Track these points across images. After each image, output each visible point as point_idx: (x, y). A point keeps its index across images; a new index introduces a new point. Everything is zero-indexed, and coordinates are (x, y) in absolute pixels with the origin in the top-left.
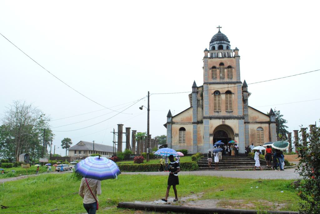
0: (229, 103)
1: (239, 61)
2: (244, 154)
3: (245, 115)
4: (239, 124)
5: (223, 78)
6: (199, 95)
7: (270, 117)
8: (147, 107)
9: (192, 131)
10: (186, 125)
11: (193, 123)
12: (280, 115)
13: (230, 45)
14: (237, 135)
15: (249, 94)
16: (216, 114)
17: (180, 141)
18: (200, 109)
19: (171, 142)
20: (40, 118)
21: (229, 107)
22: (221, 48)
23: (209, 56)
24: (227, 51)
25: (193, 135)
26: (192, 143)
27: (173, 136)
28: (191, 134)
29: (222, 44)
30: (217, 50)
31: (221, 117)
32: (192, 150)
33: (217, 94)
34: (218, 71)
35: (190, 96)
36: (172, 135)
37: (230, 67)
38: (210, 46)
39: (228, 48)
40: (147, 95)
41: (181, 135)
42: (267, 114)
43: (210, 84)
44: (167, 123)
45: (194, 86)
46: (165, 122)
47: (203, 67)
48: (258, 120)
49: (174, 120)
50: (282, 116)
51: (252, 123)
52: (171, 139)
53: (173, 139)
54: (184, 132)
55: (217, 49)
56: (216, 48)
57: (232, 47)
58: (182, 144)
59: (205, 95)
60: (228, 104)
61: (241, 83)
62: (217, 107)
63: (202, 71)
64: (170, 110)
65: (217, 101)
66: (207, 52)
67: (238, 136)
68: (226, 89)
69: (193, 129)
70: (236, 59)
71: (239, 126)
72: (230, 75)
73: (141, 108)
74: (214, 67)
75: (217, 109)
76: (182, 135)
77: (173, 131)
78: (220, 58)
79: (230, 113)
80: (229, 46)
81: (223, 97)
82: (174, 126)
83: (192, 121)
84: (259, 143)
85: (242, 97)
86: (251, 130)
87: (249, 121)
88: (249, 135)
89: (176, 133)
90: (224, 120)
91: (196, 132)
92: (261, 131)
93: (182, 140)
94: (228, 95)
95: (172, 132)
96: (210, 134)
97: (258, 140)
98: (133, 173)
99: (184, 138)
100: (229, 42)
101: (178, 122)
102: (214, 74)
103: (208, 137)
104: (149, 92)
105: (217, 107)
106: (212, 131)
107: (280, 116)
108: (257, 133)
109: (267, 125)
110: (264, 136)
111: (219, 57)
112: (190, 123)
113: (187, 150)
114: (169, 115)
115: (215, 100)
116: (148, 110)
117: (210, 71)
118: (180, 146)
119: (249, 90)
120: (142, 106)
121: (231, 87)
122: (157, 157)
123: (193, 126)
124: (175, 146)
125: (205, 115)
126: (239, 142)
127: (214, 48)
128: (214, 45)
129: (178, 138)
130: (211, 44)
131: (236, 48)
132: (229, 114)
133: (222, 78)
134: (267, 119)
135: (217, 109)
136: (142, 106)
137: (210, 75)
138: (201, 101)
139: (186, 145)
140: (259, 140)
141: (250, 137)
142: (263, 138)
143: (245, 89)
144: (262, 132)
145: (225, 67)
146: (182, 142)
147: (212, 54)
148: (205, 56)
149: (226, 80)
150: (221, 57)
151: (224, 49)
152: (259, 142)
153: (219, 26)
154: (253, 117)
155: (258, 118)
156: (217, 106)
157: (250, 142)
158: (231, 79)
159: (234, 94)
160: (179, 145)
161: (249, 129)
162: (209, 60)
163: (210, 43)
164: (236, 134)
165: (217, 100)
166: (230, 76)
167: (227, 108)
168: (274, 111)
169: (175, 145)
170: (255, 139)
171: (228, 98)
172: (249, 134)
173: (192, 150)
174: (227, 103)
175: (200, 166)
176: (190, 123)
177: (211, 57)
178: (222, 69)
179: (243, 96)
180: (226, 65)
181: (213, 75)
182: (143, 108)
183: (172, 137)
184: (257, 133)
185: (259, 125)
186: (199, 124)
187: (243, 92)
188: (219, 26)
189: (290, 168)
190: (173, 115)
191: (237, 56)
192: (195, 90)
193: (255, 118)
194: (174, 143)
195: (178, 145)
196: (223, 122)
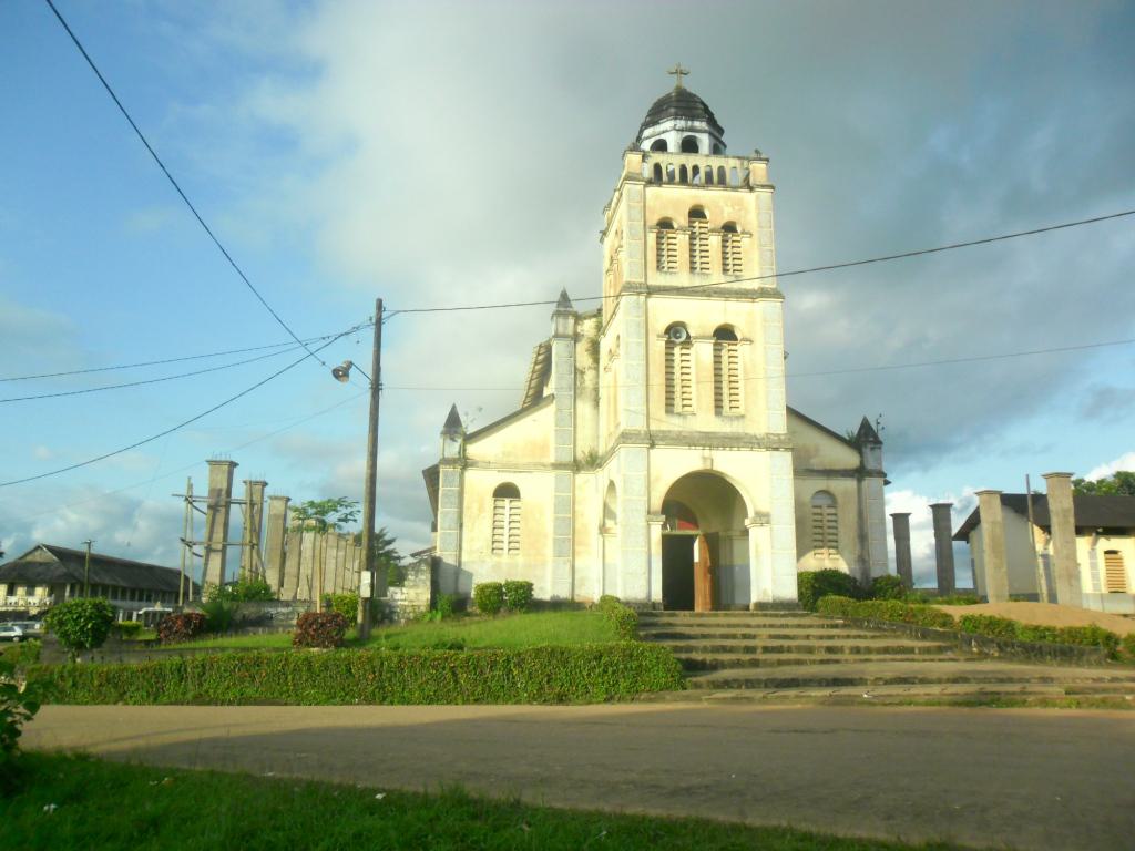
6: (582, 346)
7: (861, 453)
8: (370, 373)
11: (557, 466)
13: (725, 147)
14: (763, 518)
16: (674, 424)
18: (584, 408)
26: (549, 550)
29: (697, 135)
34: (682, 240)
37: (729, 228)
40: (373, 312)
41: (497, 517)
43: (651, 291)
54: (515, 504)
58: (505, 559)
64: (454, 407)
70: (758, 198)
74: (665, 224)
76: (507, 519)
79: (735, 423)
81: (703, 352)
82: (470, 474)
83: (552, 459)
89: (481, 509)
90: (707, 452)
92: (829, 507)
93: (506, 539)
96: (649, 513)
101: (487, 459)
108: (815, 514)
109: (851, 484)
112: (544, 466)
114: (453, 424)
116: (376, 387)
117: (652, 237)
118: (497, 567)
126: (772, 547)
136: (350, 364)
138: (589, 376)
139: (520, 559)
142: (834, 537)
144: (832, 511)
146: (505, 546)
149: (716, 277)
159: (746, 340)
160: (491, 560)
164: (759, 515)
168: (874, 425)
169: (473, 562)
180: (715, 218)
182: (352, 371)
183: (461, 526)
184: (815, 514)
185: (821, 484)
192: (566, 328)
195: (488, 560)
196: (704, 458)
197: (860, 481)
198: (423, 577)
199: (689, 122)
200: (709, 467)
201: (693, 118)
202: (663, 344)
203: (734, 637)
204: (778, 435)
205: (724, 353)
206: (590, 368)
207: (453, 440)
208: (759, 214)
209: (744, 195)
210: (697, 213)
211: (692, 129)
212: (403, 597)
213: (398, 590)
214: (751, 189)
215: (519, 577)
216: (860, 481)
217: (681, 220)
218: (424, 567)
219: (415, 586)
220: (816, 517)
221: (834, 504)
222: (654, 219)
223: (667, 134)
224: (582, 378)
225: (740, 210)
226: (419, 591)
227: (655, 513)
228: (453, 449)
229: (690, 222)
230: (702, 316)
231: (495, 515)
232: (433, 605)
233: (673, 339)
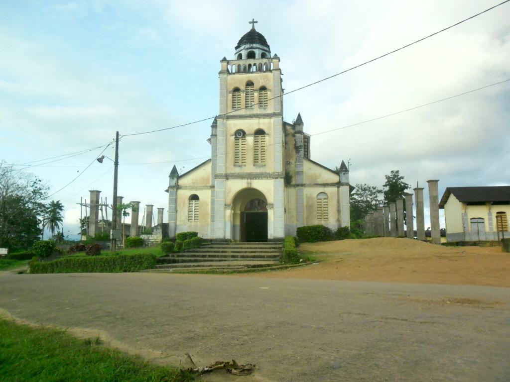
3: (297, 172)
4: (275, 186)
8: (114, 160)
9: (209, 201)
10: (200, 191)
14: (272, 205)
16: (237, 170)
19: (176, 219)
20: (33, 186)
22: (251, 55)
27: (178, 209)
28: (207, 205)
32: (209, 233)
34: (243, 95)
37: (263, 88)
41: (190, 208)
43: (228, 118)
48: (319, 181)
50: (402, 178)
51: (310, 185)
53: (179, 214)
54: (196, 202)
55: (245, 58)
56: (244, 57)
64: (175, 166)
66: (225, 64)
68: (256, 127)
70: (274, 74)
71: (274, 190)
73: (100, 160)
74: (237, 90)
75: (240, 161)
76: (194, 208)
77: (179, 201)
79: (262, 168)
80: (267, 53)
81: (250, 140)
82: (180, 192)
86: (306, 197)
87: (304, 183)
88: (303, 206)
89: (184, 204)
90: (249, 181)
92: (325, 199)
93: (193, 215)
94: (260, 137)
96: (225, 205)
97: (318, 214)
98: (101, 274)
99: (197, 213)
100: (268, 46)
101: (186, 186)
103: (222, 209)
104: (117, 133)
106: (230, 198)
107: (400, 179)
109: (335, 189)
110: (329, 207)
114: (174, 173)
115: (237, 145)
116: (116, 164)
117: (230, 96)
118: (190, 226)
120: (103, 157)
121: (263, 124)
122: (148, 244)
126: (274, 217)
127: (240, 57)
128: (241, 52)
129: (187, 213)
134: (335, 178)
135: (237, 160)
136: (103, 157)
137: (230, 104)
144: (326, 200)
145: (254, 88)
146: (193, 218)
149: (257, 110)
150: (255, 70)
152: (321, 217)
153: (253, 20)
158: (265, 109)
159: (268, 135)
160: (188, 224)
161: (305, 195)
168: (346, 164)
170: (315, 213)
172: (303, 203)
173: (209, 233)
174: (256, 149)
176: (205, 187)
180: (257, 86)
183: (177, 211)
185: (321, 189)
188: (253, 20)
189: (300, 265)
190: (180, 173)
196: (248, 183)
197: (338, 187)
199: (251, 45)
200: (249, 186)
201: (252, 43)
202: (233, 138)
203: (218, 252)
205: (260, 141)
207: (173, 179)
208: (274, 82)
209: (269, 74)
210: (250, 84)
211: (252, 48)
212: (152, 238)
213: (150, 236)
214: (271, 71)
216: (338, 187)
217: (242, 87)
218: (159, 227)
219: (156, 234)
220: (318, 204)
222: (231, 88)
226: (158, 236)
227: (229, 205)
229: (246, 87)
233: (238, 136)
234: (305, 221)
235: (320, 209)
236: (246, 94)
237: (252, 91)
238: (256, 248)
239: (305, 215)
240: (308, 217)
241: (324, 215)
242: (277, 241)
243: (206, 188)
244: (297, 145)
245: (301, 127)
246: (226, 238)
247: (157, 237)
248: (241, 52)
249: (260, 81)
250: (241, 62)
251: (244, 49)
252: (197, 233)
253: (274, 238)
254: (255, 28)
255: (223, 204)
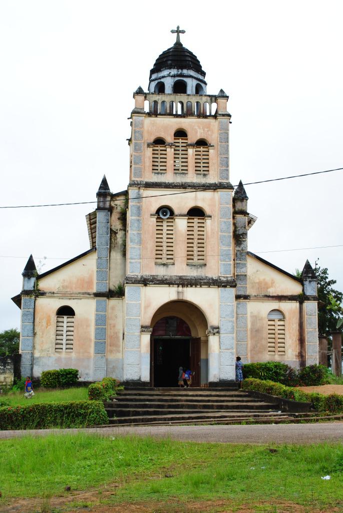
0: (196, 241)
1: (228, 130)
2: (232, 381)
3: (237, 275)
5: (184, 172)
6: (115, 216)
7: (303, 285)
10: (75, 300)
11: (97, 295)
12: (327, 280)
13: (206, 84)
14: (217, 330)
15: (250, 222)
16: (161, 272)
17: (58, 347)
18: (116, 256)
19: (34, 347)
21: (195, 253)
22: (179, 88)
23: (147, 110)
24: (198, 98)
25: (96, 329)
27: (37, 329)
28: (88, 326)
29: (185, 79)
30: (169, 94)
31: (174, 278)
32: (91, 372)
33: (165, 216)
35: (92, 219)
36: (36, 328)
37: (202, 143)
38: (151, 81)
39: (199, 89)
42: (295, 274)
43: (149, 185)
44: (21, 293)
45: (104, 191)
46: (18, 292)
47: (130, 140)
48: (272, 291)
49: (43, 285)
50: (334, 282)
51: (257, 298)
52: (34, 339)
54: (70, 320)
56: (168, 88)
57: (211, 89)
58: (64, 355)
59: (131, 216)
60: (195, 245)
61: (231, 187)
62: (164, 252)
63: (126, 151)
64: (31, 257)
65: (165, 236)
66: (141, 98)
67: (218, 332)
68: (191, 204)
69: (97, 310)
72: (202, 165)
74: (159, 141)
75: (164, 256)
76: (65, 329)
78: (177, 116)
79: (200, 270)
80: (203, 85)
81: (181, 224)
82: (41, 301)
83: (94, 290)
84: (274, 352)
85: (232, 228)
86: (252, 317)
87: (248, 293)
90: (180, 289)
91: (102, 321)
92: (280, 320)
93: (64, 342)
94: (196, 220)
95: (37, 320)
96: (142, 327)
97: (269, 345)
100: (203, 74)
102: (159, 160)
105: (164, 252)
106: (147, 318)
107: (330, 283)
109: (295, 305)
110: (287, 332)
111: (174, 113)
112: (89, 294)
113: (77, 368)
117: (149, 152)
118: (58, 360)
119: (251, 207)
121: (202, 199)
123: (97, 305)
124: (44, 360)
125: (129, 273)
127: (161, 88)
128: (162, 80)
130: (154, 77)
131: (222, 91)
132: (195, 271)
133: (180, 171)
134: (295, 289)
137: (148, 163)
138: (120, 235)
139: (73, 355)
140: (273, 345)
141: (249, 336)
143: (239, 206)
144: (282, 323)
145: (189, 142)
146: (64, 347)
147: (156, 102)
148: (136, 108)
149: (191, 178)
150: (180, 112)
151: (189, 92)
153: (178, 28)
154: (260, 283)
155: (272, 286)
156: (165, 248)
157: (249, 350)
159: (210, 217)
161: (249, 315)
162: (148, 121)
163: (153, 72)
164: (214, 328)
165: (165, 232)
166: (202, 169)
167: (190, 257)
168: (313, 267)
169: (43, 357)
171: (196, 228)
173: (91, 372)
174: (190, 239)
175: (110, 414)
177: (153, 113)
178: (181, 149)
179: (234, 224)
180: (192, 138)
181: (156, 164)
183: (35, 334)
185: (275, 305)
186: (111, 297)
187: (236, 213)
188: (178, 28)
190: (41, 269)
191: (223, 115)
193: (263, 285)
194: (42, 351)
195: (52, 355)
197: (301, 303)
198: (9, 367)
199: (180, 71)
200: (181, 298)
201: (182, 67)
202: (155, 219)
204: (227, 277)
205: (196, 225)
206: (120, 230)
210: (181, 133)
211: (181, 75)
215: (72, 367)
216: (301, 303)
221: (283, 319)
223: (165, 78)
224: (116, 236)
225: (208, 131)
226: (6, 376)
227: (146, 327)
228: (30, 285)
229: (175, 139)
230: (181, 201)
231: (57, 326)
232: (15, 383)
233: (161, 216)
234: (249, 354)
235: (273, 336)
236: (175, 150)
237: (185, 145)
238: (211, 396)
239: (249, 345)
240: (253, 348)
241: (278, 344)
242: (223, 385)
243: (89, 296)
244: (237, 232)
245: (244, 203)
246: (143, 380)
247: (5, 378)
248: (162, 80)
249: (199, 130)
250: (159, 98)
251: (169, 75)
252: (77, 371)
253: (220, 381)
254: (182, 41)
255: (139, 325)
